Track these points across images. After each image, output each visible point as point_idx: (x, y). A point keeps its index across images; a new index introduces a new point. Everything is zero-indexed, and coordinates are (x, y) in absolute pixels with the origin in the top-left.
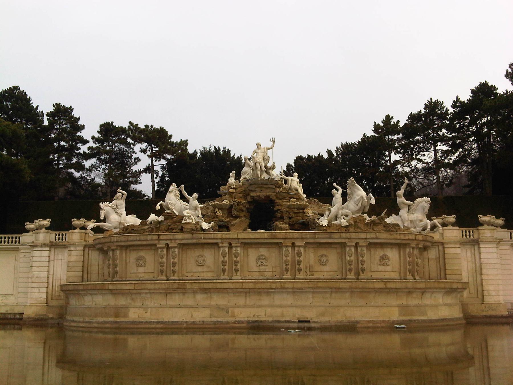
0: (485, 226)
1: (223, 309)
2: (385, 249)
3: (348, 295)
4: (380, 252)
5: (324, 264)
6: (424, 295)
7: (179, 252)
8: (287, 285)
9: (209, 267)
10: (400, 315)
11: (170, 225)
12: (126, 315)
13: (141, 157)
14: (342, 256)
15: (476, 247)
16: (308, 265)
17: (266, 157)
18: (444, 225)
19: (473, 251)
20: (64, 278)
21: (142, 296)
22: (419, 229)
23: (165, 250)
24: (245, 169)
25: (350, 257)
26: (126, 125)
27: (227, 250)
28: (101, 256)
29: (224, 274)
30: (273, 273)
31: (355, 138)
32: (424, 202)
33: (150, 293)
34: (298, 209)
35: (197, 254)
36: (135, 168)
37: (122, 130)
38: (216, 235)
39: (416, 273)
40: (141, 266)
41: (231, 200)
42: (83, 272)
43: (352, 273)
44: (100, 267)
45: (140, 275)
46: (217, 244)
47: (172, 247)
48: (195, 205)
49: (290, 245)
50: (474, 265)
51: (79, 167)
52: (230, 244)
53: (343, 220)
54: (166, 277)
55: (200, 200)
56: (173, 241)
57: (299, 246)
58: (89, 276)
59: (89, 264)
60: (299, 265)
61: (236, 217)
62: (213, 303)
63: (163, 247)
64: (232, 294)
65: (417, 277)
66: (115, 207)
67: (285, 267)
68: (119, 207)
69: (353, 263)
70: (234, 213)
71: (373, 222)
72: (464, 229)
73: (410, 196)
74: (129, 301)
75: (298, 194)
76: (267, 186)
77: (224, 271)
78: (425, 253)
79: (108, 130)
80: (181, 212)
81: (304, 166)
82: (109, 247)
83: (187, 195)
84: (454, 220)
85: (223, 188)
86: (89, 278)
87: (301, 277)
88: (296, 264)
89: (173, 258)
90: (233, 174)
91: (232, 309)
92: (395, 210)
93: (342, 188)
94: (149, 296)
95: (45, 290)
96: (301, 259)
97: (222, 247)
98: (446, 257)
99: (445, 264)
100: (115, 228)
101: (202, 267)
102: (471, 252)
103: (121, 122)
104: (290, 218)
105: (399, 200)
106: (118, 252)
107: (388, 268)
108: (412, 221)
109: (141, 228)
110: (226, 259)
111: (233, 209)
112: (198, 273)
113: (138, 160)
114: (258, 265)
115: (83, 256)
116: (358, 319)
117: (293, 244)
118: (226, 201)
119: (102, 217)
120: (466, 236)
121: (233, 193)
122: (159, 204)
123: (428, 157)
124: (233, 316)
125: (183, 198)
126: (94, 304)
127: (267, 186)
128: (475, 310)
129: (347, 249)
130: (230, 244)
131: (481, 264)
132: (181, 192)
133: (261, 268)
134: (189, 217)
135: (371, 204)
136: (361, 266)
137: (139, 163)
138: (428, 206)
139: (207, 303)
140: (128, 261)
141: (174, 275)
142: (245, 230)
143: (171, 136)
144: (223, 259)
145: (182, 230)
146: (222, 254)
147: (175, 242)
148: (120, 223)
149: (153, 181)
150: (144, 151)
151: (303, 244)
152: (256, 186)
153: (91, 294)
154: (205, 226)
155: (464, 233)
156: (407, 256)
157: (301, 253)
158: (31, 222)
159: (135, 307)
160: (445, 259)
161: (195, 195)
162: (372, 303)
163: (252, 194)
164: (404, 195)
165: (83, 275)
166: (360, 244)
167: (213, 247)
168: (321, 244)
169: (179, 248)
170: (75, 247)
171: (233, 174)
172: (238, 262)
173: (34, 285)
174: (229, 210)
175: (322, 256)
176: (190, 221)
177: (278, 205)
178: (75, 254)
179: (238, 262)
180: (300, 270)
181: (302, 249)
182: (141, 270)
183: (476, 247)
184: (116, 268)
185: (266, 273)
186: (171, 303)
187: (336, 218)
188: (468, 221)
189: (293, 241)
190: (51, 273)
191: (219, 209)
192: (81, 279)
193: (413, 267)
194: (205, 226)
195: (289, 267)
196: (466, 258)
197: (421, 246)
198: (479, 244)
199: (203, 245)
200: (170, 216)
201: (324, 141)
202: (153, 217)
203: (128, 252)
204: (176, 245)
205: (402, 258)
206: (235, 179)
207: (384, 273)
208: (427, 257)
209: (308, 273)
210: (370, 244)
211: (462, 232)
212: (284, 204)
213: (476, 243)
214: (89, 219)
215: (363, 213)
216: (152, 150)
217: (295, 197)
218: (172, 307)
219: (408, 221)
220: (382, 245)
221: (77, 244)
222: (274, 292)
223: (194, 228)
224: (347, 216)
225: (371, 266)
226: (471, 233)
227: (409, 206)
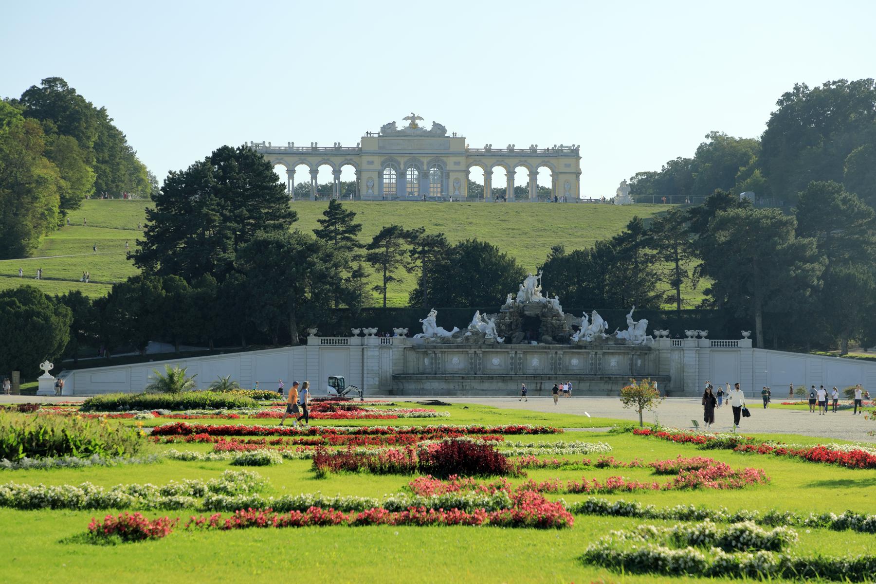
18: (661, 337)
22: (639, 342)
24: (520, 293)
32: (644, 323)
70: (513, 327)
71: (607, 338)
73: (636, 318)
80: (484, 329)
85: (503, 307)
92: (626, 327)
95: (377, 379)
105: (628, 321)
125: (483, 320)
138: (645, 326)
158: (356, 328)
164: (633, 317)
171: (510, 296)
187: (584, 336)
194: (500, 340)
200: (475, 333)
202: (456, 329)
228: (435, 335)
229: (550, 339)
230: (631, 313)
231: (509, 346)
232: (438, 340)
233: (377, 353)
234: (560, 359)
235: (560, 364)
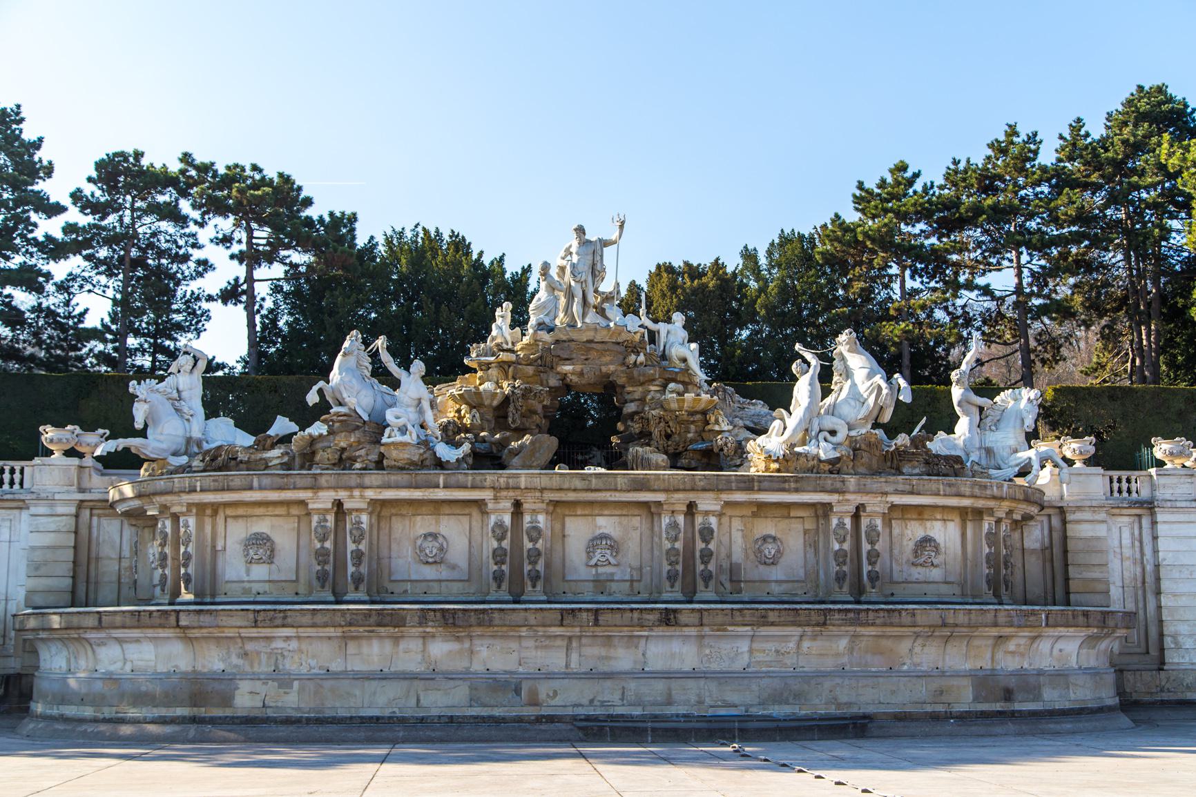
2: (928, 524)
4: (914, 531)
6: (1035, 645)
7: (371, 526)
9: (453, 567)
10: (976, 699)
11: (343, 450)
12: (227, 700)
13: (214, 253)
16: (726, 565)
17: (599, 267)
19: (1137, 532)
20: (21, 595)
21: (274, 645)
23: (331, 518)
26: (175, 167)
27: (507, 519)
28: (128, 532)
29: (499, 587)
30: (631, 586)
31: (808, 220)
33: (299, 638)
35: (422, 532)
36: (194, 286)
37: (162, 180)
38: (478, 478)
40: (260, 561)
41: (505, 384)
42: (73, 577)
43: (846, 588)
44: (125, 564)
45: (256, 587)
46: (480, 504)
47: (351, 511)
48: (416, 396)
49: (685, 508)
50: (1139, 570)
51: (30, 279)
52: (517, 505)
53: (823, 444)
54: (334, 593)
55: (431, 379)
56: (356, 493)
57: (707, 513)
58: (92, 587)
59: (93, 555)
60: (705, 563)
61: (520, 432)
62: (477, 667)
63: (327, 510)
64: (530, 643)
65: (1005, 598)
66: (175, 395)
67: (666, 567)
68: (184, 395)
69: (848, 560)
70: (513, 418)
72: (1115, 474)
74: (235, 660)
75: (687, 370)
76: (599, 347)
79: (120, 173)
81: (704, 298)
82: (164, 508)
84: (1092, 450)
86: (92, 596)
87: (711, 595)
88: (698, 561)
89: (531, 540)
90: (503, 314)
91: (530, 683)
93: (821, 357)
94: (294, 644)
96: (712, 546)
97: (495, 511)
98: (1071, 545)
99: (1067, 565)
100: (175, 454)
101: (434, 567)
102: (1133, 534)
103: (162, 156)
104: (668, 437)
105: (957, 393)
106: (192, 521)
108: (989, 452)
109: (259, 456)
110: (506, 544)
111: (511, 408)
112: (424, 584)
113: (205, 265)
114: (593, 562)
115: (76, 533)
116: (870, 709)
117: (691, 508)
118: (488, 386)
119: (139, 425)
120: (1120, 491)
121: (509, 364)
122: (315, 388)
123: (1003, 280)
124: (534, 703)
126: (128, 668)
128: (1140, 685)
130: (517, 505)
131: (1157, 566)
132: (375, 355)
133: (600, 570)
134: (403, 430)
135: (898, 402)
136: (866, 568)
137: (209, 275)
139: (460, 665)
140: (219, 548)
141: (357, 589)
142: (551, 465)
143: (308, 202)
144: (495, 544)
145: (379, 465)
146: (493, 531)
147: (362, 497)
148: (189, 440)
149: (251, 324)
150: (226, 240)
151: (718, 508)
152: (573, 345)
153: (120, 641)
154: (445, 452)
156: (984, 542)
157: (712, 531)
159: (255, 677)
160: (1065, 552)
162: (905, 667)
165: (74, 585)
166: (868, 509)
167: (467, 511)
168: (761, 506)
169: (371, 514)
170: (52, 506)
171: (503, 314)
172: (539, 554)
174: (500, 413)
175: (765, 539)
176: (406, 438)
177: (632, 401)
178: (53, 527)
179: (539, 554)
180: (707, 578)
181: (713, 521)
182: (260, 572)
183: (1146, 522)
184: (186, 566)
185: (614, 586)
186: (357, 665)
191: (472, 407)
192: (68, 597)
193: (997, 571)
195: (679, 568)
196: (1118, 550)
197: (1017, 517)
198: (1153, 514)
201: (730, 229)
202: (282, 425)
203: (220, 519)
204: (364, 506)
206: (512, 327)
207: (926, 588)
208: (1018, 545)
209: (728, 585)
210: (893, 507)
211: (1111, 482)
212: (649, 397)
214: (88, 427)
215: (876, 425)
216: (250, 237)
217: (679, 378)
219: (980, 448)
220: (920, 512)
221: (57, 497)
222: (647, 637)
223: (416, 458)
225: (891, 570)
227: (981, 409)
228: (190, 445)
229: (661, 458)
231: (491, 476)
232: (196, 463)
234: (707, 534)
235: (707, 556)
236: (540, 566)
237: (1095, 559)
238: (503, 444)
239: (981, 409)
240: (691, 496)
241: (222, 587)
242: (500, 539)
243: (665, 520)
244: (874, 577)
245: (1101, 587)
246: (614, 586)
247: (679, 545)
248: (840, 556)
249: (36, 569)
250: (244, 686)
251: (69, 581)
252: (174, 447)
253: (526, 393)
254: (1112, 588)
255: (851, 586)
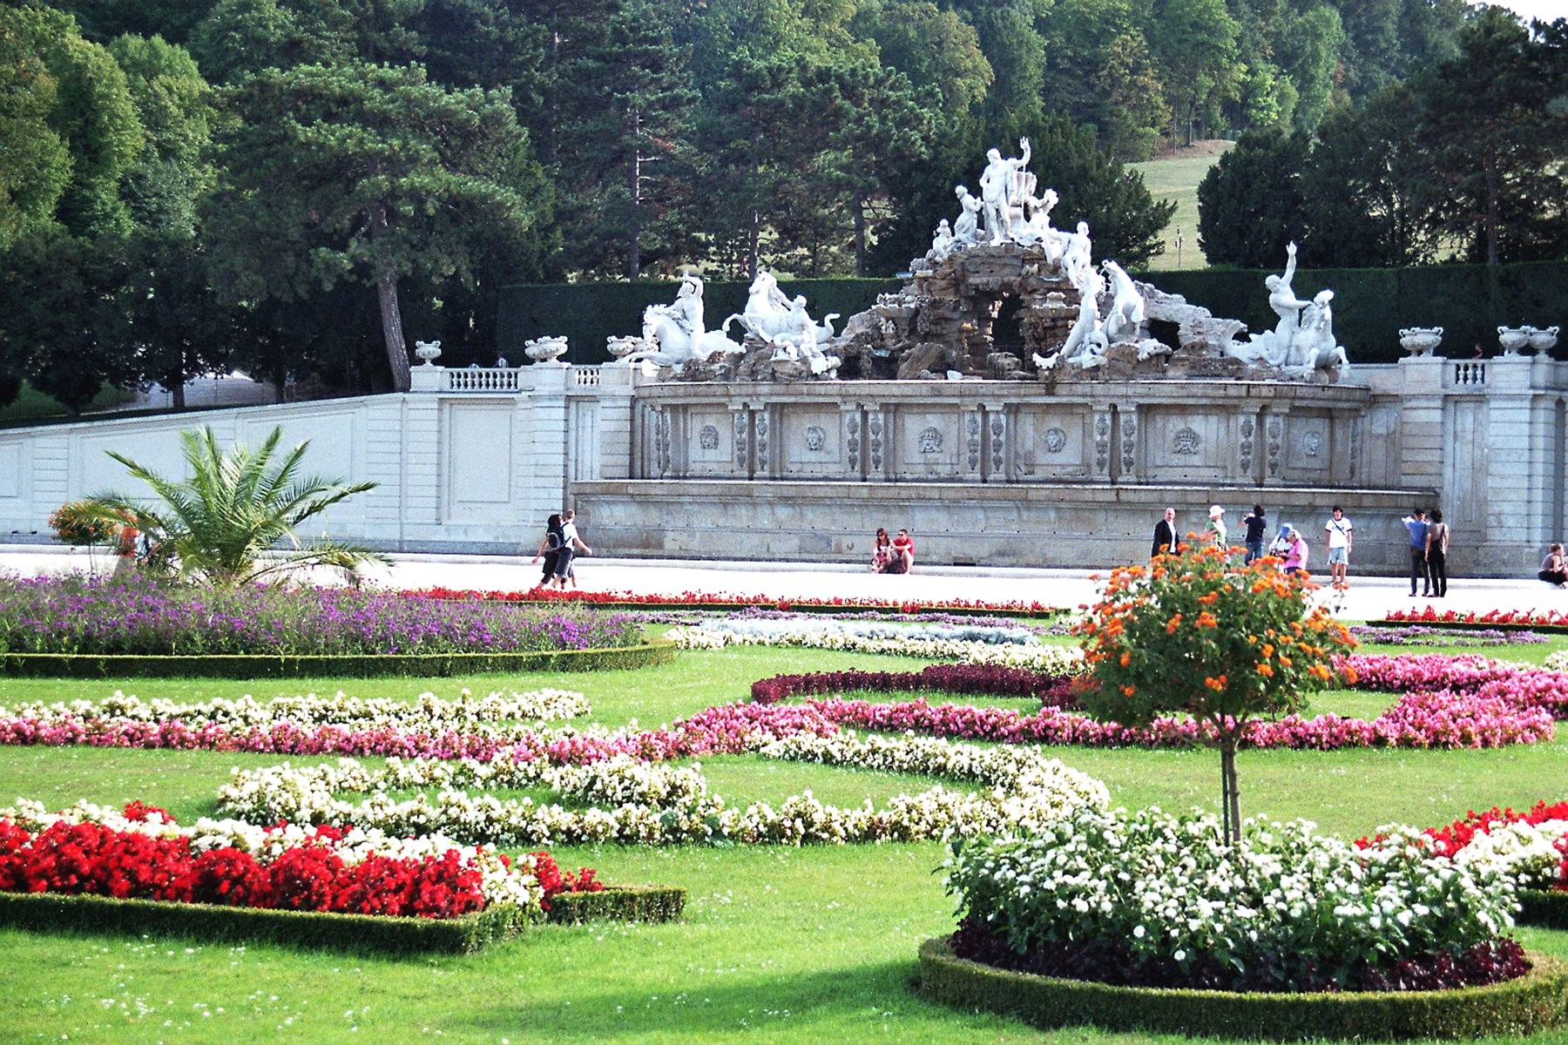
0: (1511, 357)
1: (822, 538)
3: (1052, 515)
4: (1176, 424)
5: (1057, 449)
7: (772, 421)
8: (928, 494)
12: (660, 545)
14: (1087, 434)
15: (1485, 407)
25: (1103, 434)
34: (1054, 320)
39: (1268, 471)
42: (631, 455)
43: (1106, 471)
57: (997, 412)
65: (1267, 481)
66: (678, 315)
70: (921, 327)
72: (1462, 362)
77: (852, 462)
78: (1364, 424)
83: (787, 301)
85: (915, 262)
92: (1262, 318)
94: (696, 508)
95: (559, 493)
96: (1002, 438)
105: (1272, 297)
107: (1196, 460)
108: (1298, 348)
120: (1466, 379)
121: (926, 279)
127: (1003, 261)
129: (1097, 417)
154: (819, 365)
155: (1462, 372)
161: (801, 300)
163: (971, 280)
164: (1293, 285)
172: (878, 444)
173: (540, 482)
180: (998, 462)
182: (711, 454)
186: (732, 522)
188: (1470, 342)
189: (979, 400)
190: (572, 456)
195: (978, 454)
199: (819, 407)
205: (1233, 438)
210: (1140, 406)
213: (1481, 399)
218: (734, 531)
219: (1289, 347)
220: (1183, 410)
224: (1099, 345)
226: (1479, 372)
230: (1290, 272)
233: (561, 413)
234: (998, 429)
235: (998, 445)
236: (881, 453)
237: (1430, 443)
238: (902, 350)
239: (1301, 311)
240: (979, 400)
241: (692, 466)
242: (853, 433)
243: (967, 417)
244: (1129, 463)
245: (1432, 470)
246: (939, 469)
247: (978, 437)
248: (1101, 447)
249: (608, 447)
250: (670, 535)
251: (627, 459)
252: (678, 356)
253: (934, 304)
254: (1448, 471)
255: (1111, 469)
